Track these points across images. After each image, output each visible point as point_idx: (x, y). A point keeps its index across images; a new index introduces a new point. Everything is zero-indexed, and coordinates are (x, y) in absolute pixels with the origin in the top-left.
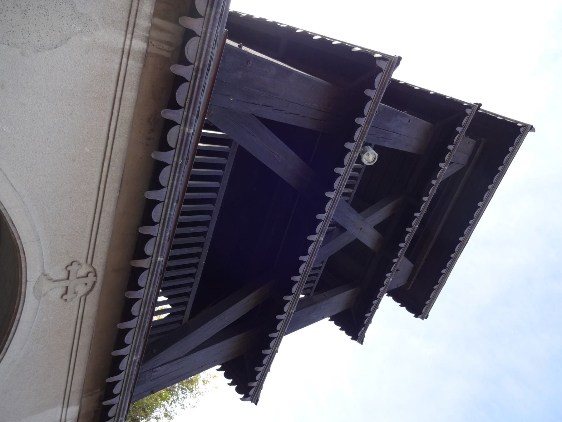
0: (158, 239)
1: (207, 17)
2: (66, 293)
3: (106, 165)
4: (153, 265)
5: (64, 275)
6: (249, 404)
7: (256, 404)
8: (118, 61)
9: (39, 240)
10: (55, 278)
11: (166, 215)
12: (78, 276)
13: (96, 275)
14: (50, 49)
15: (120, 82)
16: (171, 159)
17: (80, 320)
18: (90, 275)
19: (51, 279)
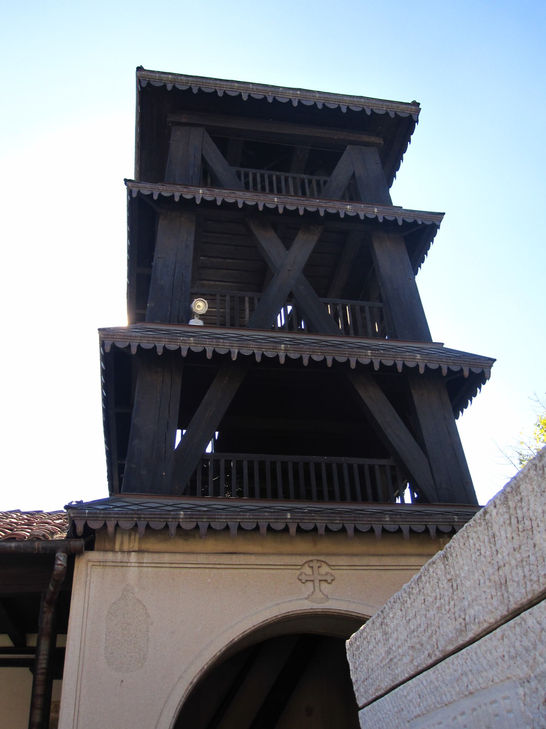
0: (271, 521)
1: (104, 519)
2: (326, 581)
3: (219, 566)
4: (294, 521)
5: (310, 584)
7: (495, 360)
8: (146, 569)
9: (278, 604)
10: (312, 590)
11: (250, 519)
12: (312, 573)
13: (312, 561)
14: (146, 609)
15: (159, 565)
19: (313, 593)
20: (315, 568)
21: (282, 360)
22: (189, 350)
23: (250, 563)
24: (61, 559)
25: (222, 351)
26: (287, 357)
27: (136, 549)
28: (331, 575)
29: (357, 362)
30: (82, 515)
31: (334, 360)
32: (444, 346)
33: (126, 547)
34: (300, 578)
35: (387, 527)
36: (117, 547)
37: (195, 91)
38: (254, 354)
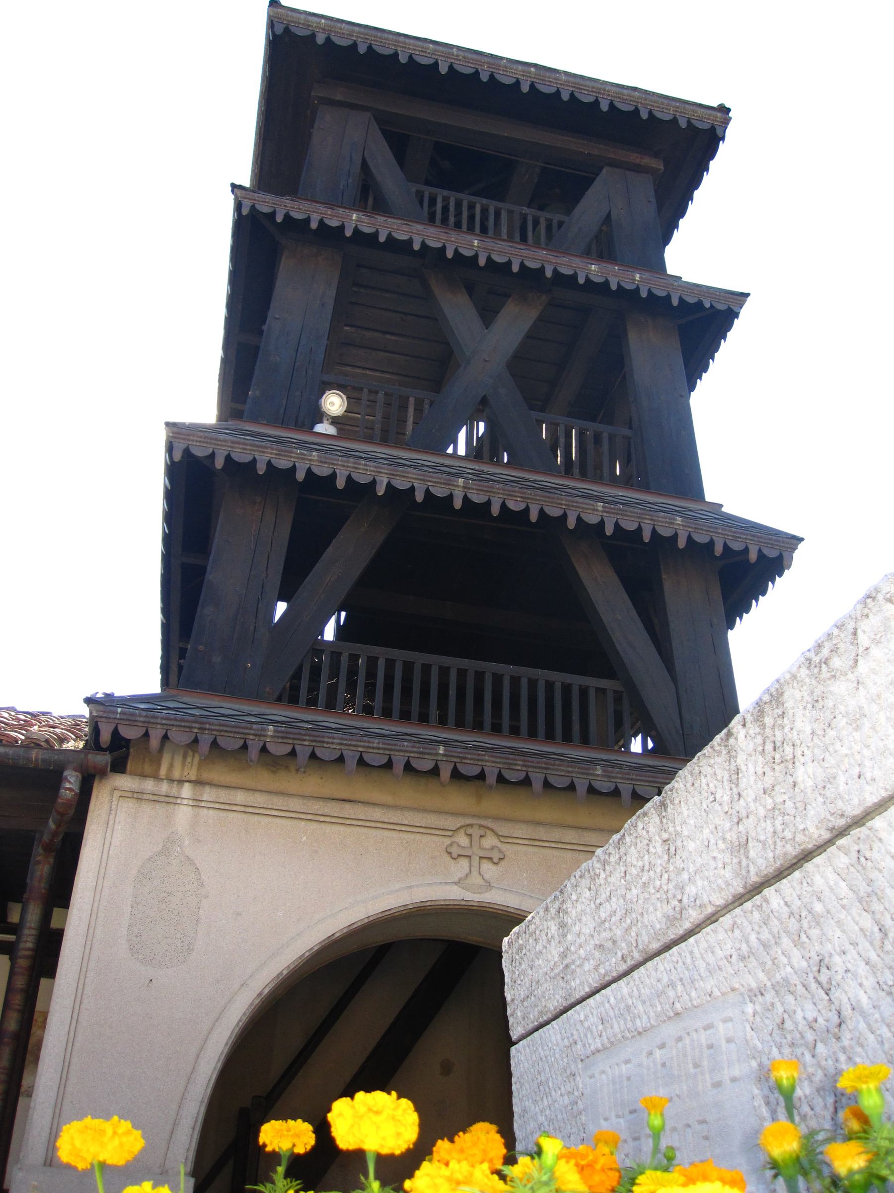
0: (412, 755)
1: (146, 725)
2: (490, 859)
3: (322, 819)
4: (449, 759)
5: (464, 862)
6: (799, 555)
7: (802, 539)
8: (205, 810)
9: (410, 887)
10: (466, 870)
11: (379, 749)
13: (471, 825)
14: (199, 874)
15: (227, 807)
16: (306, 748)
17: (533, 841)
18: (468, 832)
19: (467, 875)
20: (476, 838)
21: (458, 504)
22: (309, 472)
23: (372, 819)
24: (71, 782)
25: (363, 479)
26: (465, 498)
27: (193, 778)
28: (500, 851)
29: (579, 519)
30: (113, 716)
31: (542, 512)
32: (723, 509)
33: (176, 774)
34: (449, 850)
35: (597, 785)
36: (163, 772)
37: (362, 49)
38: (412, 489)
